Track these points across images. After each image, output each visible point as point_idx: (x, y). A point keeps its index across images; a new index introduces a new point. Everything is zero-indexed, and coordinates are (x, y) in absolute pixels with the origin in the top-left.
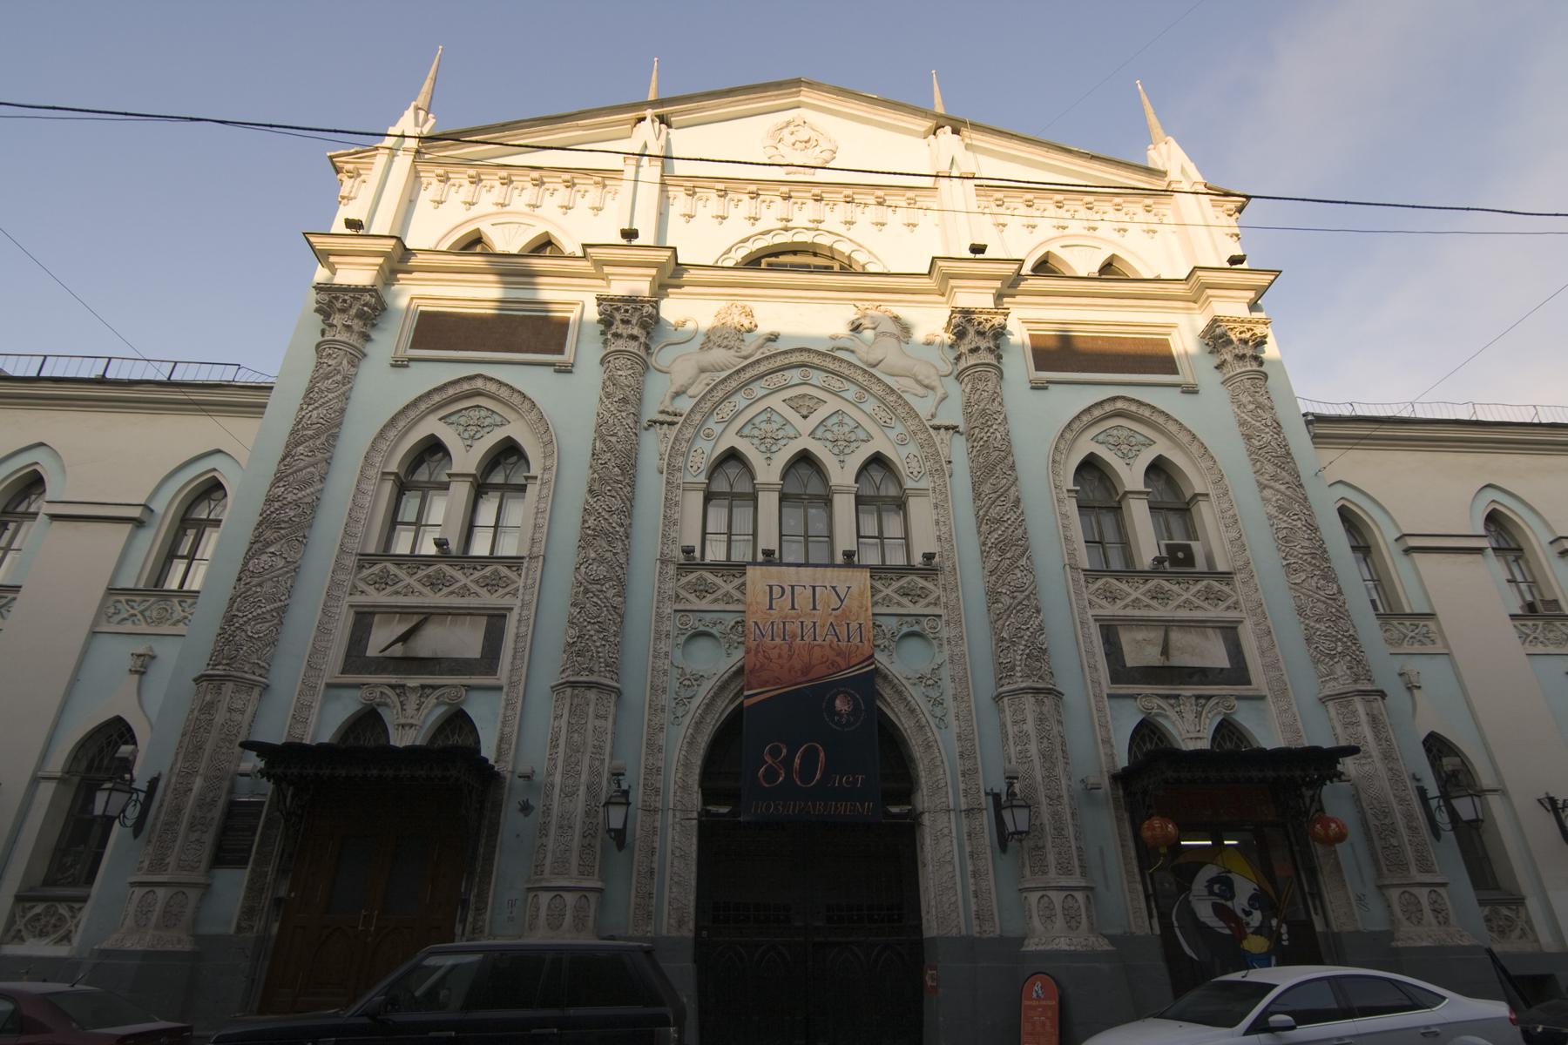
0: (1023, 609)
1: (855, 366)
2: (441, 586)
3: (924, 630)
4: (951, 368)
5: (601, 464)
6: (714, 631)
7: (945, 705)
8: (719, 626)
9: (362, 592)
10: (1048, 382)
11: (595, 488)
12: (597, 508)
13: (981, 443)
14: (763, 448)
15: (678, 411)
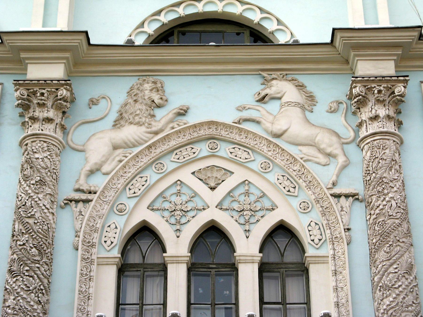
1: (261, 137)
4: (352, 134)
5: (20, 245)
11: (15, 269)
12: (16, 288)
13: (377, 211)
14: (173, 221)
15: (92, 189)
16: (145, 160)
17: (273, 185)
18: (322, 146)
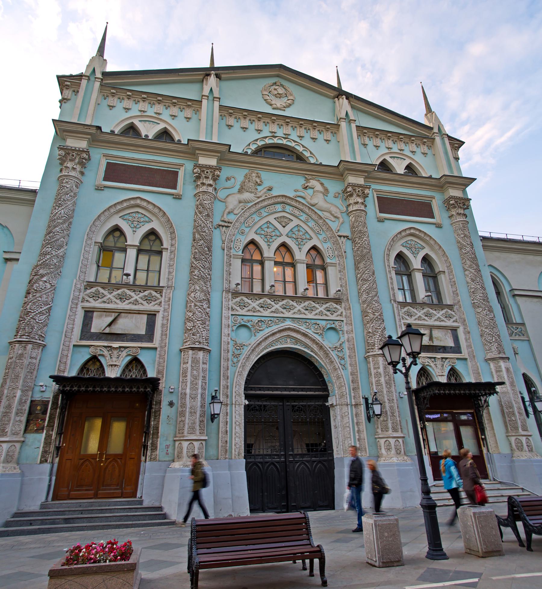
0: (377, 320)
1: (306, 205)
2: (125, 300)
3: (336, 326)
4: (345, 209)
6: (248, 324)
7: (345, 360)
8: (250, 322)
9: (87, 301)
10: (385, 219)
13: (359, 245)
15: (230, 221)
16: (253, 210)
17: (311, 228)
18: (333, 213)
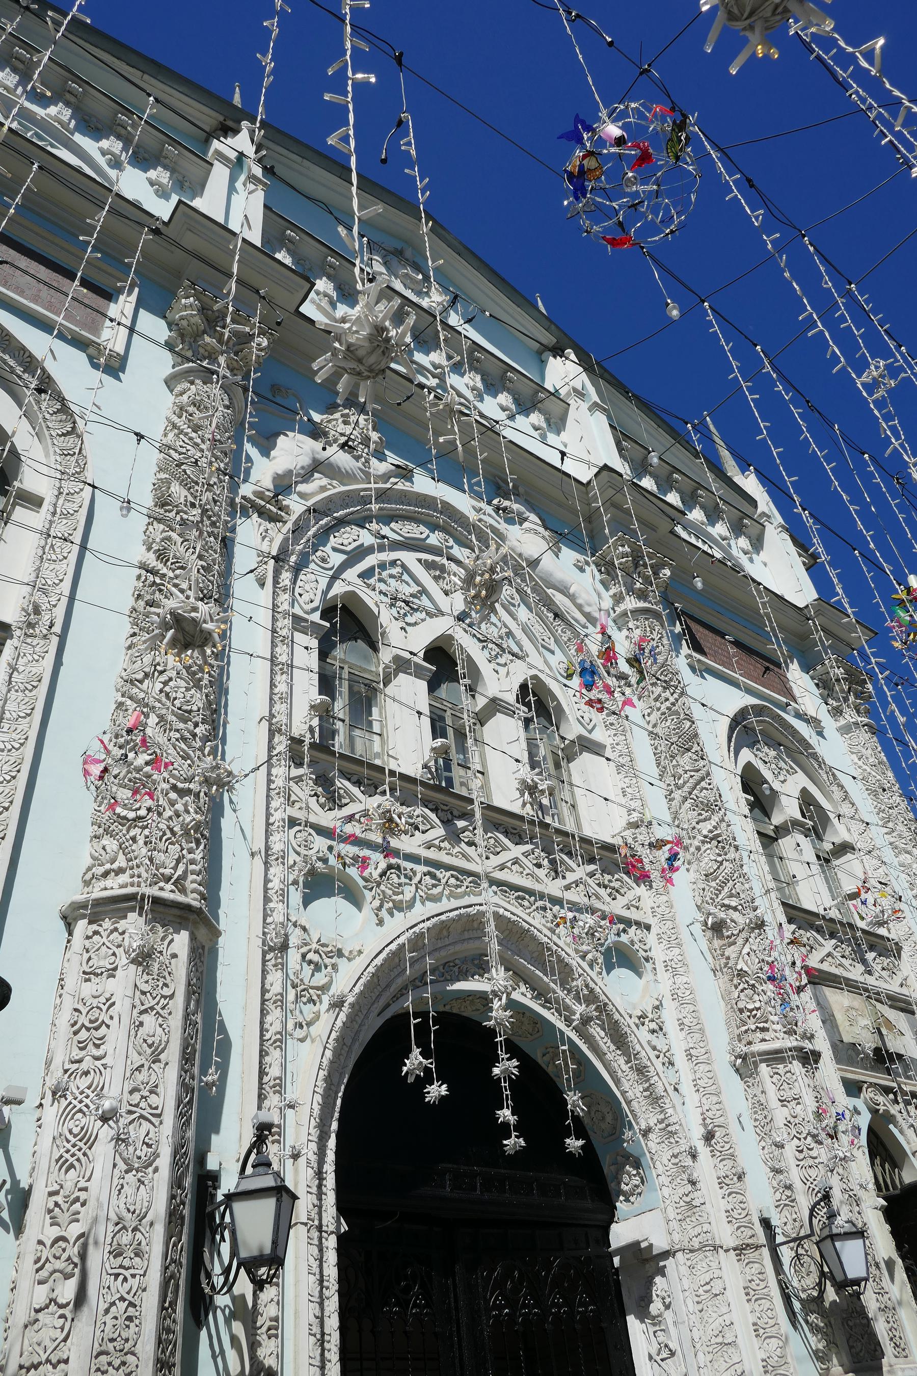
3: (632, 942)
